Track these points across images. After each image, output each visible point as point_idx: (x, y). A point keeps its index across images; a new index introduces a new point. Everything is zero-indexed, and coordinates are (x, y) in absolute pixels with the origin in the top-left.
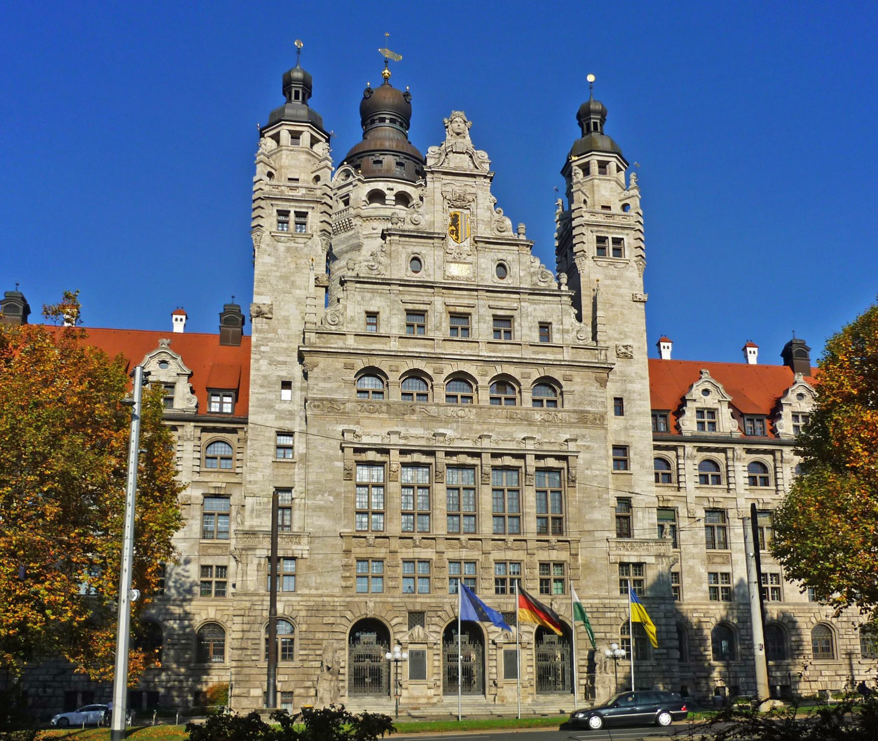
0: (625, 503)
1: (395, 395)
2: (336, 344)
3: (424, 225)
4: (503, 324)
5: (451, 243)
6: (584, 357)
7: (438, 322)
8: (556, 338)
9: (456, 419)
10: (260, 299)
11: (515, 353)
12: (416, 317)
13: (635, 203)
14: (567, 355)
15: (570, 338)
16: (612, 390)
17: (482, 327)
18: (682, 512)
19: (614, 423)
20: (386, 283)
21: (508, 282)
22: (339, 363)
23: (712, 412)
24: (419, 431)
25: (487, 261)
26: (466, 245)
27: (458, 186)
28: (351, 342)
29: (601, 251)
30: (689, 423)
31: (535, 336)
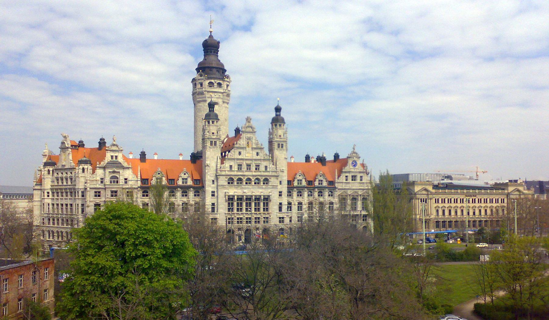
0: (281, 204)
2: (223, 173)
5: (247, 149)
6: (274, 174)
7: (244, 167)
8: (268, 170)
9: (248, 188)
12: (240, 166)
14: (270, 174)
16: (279, 179)
17: (253, 168)
18: (293, 203)
19: (279, 186)
20: (234, 159)
21: (258, 157)
22: (224, 177)
23: (301, 180)
24: (240, 191)
25: (255, 153)
26: (250, 149)
27: (249, 135)
28: (227, 173)
29: (279, 147)
30: (296, 184)
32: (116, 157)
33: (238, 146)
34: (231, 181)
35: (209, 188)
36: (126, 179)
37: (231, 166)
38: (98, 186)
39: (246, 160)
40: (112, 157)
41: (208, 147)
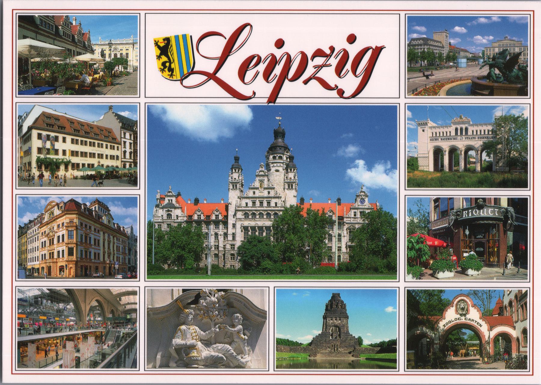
1: (250, 217)
2: (240, 209)
3: (256, 186)
4: (269, 203)
7: (258, 203)
8: (278, 205)
10: (230, 201)
11: (270, 209)
12: (254, 203)
13: (296, 178)
14: (279, 209)
15: (280, 205)
17: (265, 204)
22: (241, 212)
27: (261, 178)
28: (243, 208)
29: (289, 187)
31: (274, 205)
32: (172, 200)
33: (252, 187)
34: (246, 215)
35: (231, 221)
36: (177, 216)
37: (247, 204)
38: (159, 221)
39: (259, 198)
40: (169, 200)
41: (230, 190)
